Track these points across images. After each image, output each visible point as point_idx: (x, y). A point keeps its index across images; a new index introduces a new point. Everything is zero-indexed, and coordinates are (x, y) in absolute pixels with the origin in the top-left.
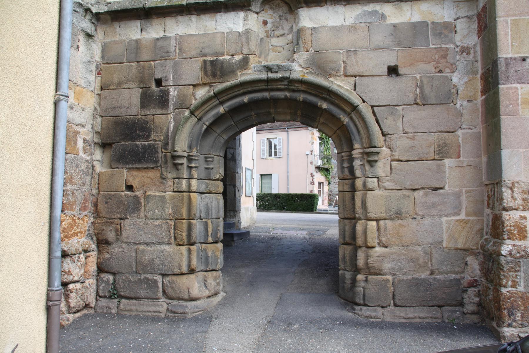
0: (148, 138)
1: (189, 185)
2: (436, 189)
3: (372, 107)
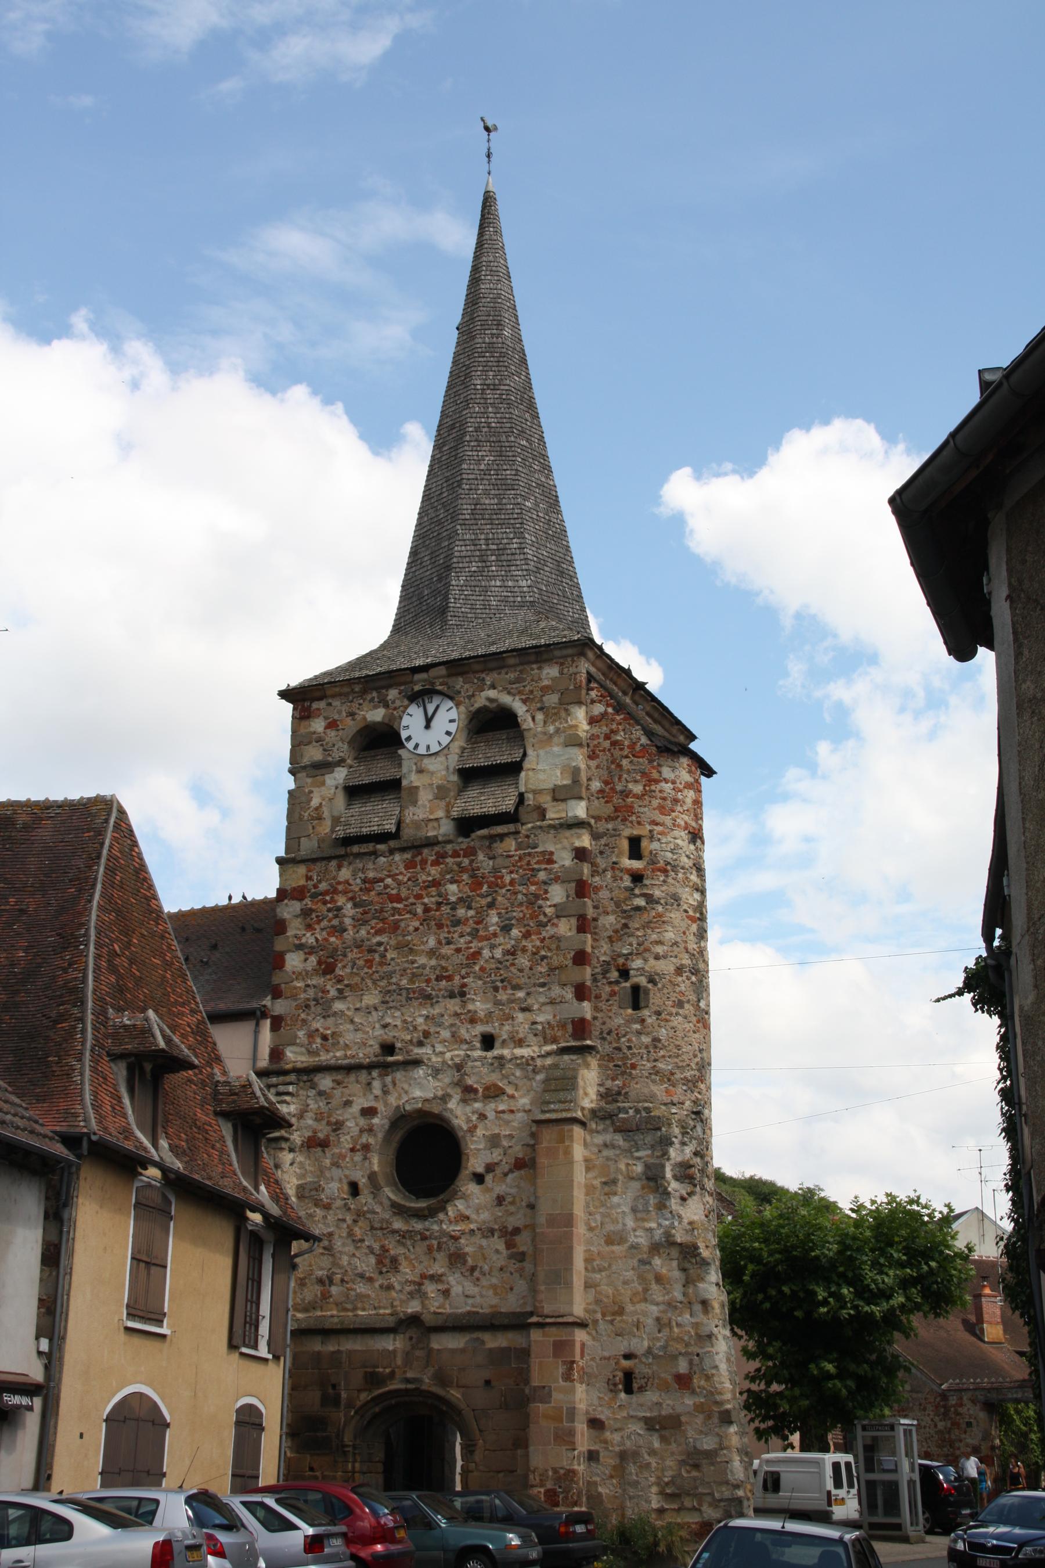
1: (353, 1467)
2: (512, 1472)
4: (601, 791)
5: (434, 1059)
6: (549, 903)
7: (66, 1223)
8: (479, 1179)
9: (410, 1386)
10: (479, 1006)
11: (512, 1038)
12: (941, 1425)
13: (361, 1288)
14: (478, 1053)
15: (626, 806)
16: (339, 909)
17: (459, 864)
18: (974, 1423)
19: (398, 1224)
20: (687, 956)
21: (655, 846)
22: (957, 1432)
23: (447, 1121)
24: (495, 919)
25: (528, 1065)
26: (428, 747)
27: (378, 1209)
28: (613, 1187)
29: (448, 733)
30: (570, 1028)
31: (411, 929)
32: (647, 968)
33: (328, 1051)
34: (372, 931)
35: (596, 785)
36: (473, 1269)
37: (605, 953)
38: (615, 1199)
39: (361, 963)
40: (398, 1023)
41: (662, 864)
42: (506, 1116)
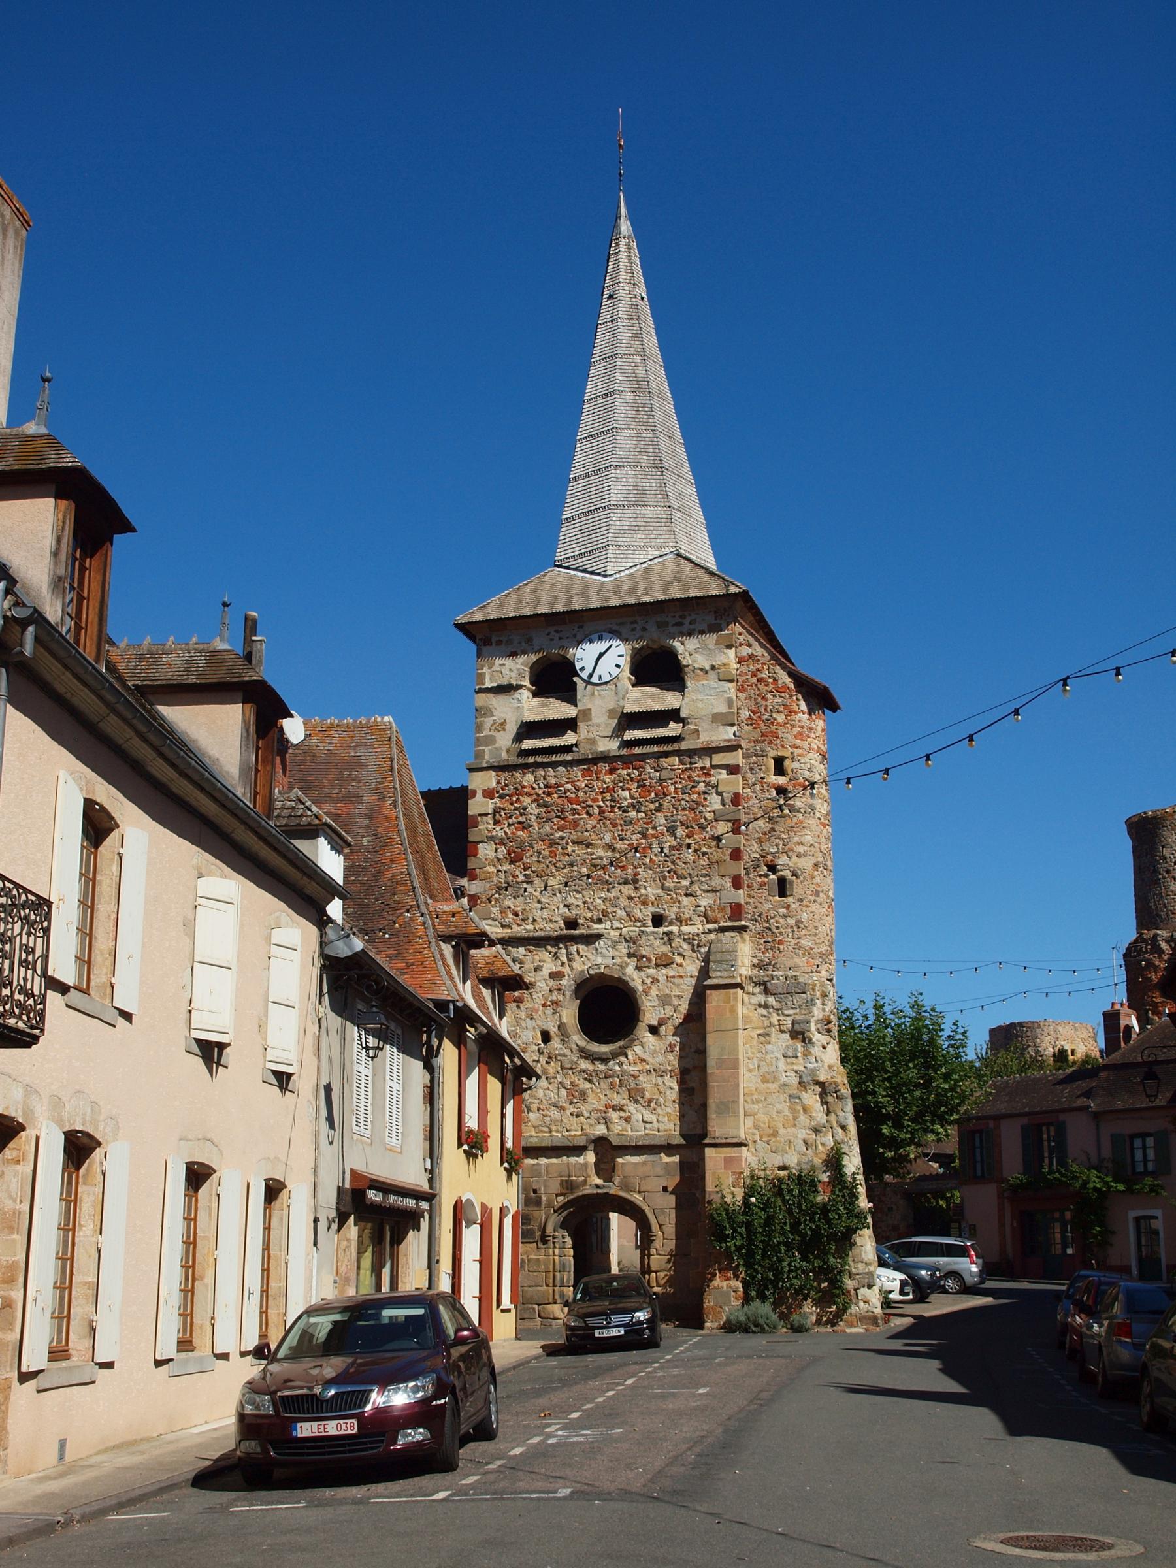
4: (750, 718)
5: (612, 933)
6: (708, 809)
7: (437, 1070)
8: (654, 1030)
9: (600, 1191)
10: (652, 891)
11: (677, 919)
13: (555, 1114)
14: (652, 929)
15: (772, 732)
16: (525, 809)
17: (628, 775)
18: (895, 1208)
19: (585, 1065)
20: (821, 854)
21: (796, 765)
23: (626, 983)
24: (663, 821)
25: (694, 939)
26: (600, 677)
27: (568, 1052)
28: (767, 1038)
29: (618, 666)
30: (729, 911)
31: (589, 827)
32: (791, 865)
33: (519, 925)
34: (555, 827)
35: (745, 714)
36: (650, 1101)
37: (756, 852)
38: (769, 1047)
39: (546, 853)
40: (581, 903)
41: (801, 780)
42: (676, 980)
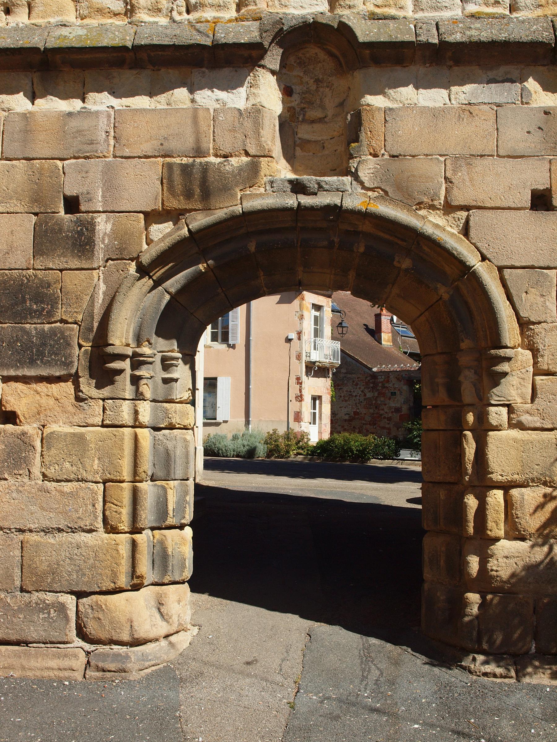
0: (49, 316)
3: (501, 269)
9: (306, 200)
12: (369, 395)
18: (398, 393)
22: (382, 399)
